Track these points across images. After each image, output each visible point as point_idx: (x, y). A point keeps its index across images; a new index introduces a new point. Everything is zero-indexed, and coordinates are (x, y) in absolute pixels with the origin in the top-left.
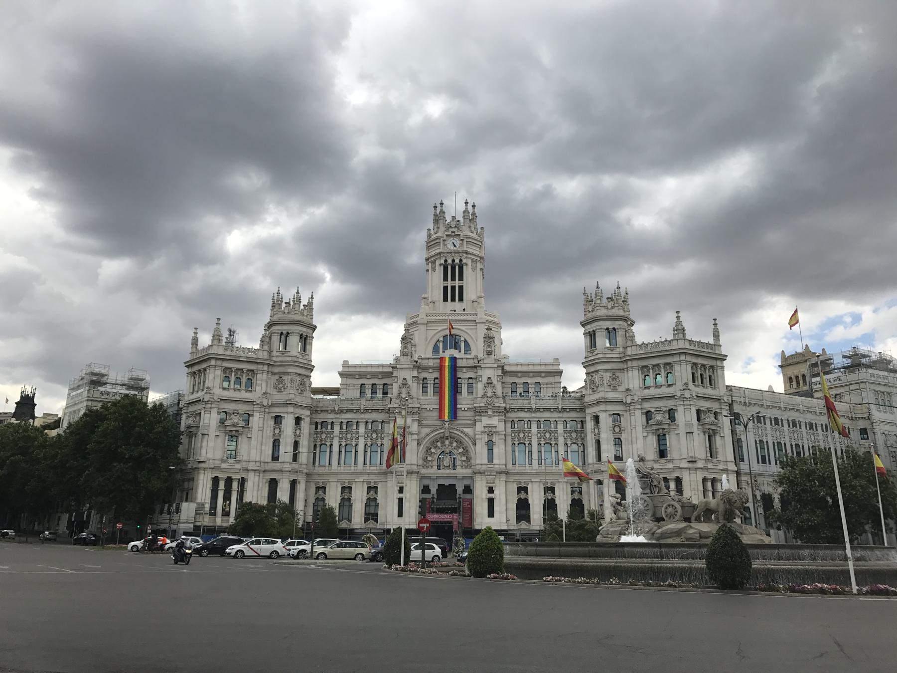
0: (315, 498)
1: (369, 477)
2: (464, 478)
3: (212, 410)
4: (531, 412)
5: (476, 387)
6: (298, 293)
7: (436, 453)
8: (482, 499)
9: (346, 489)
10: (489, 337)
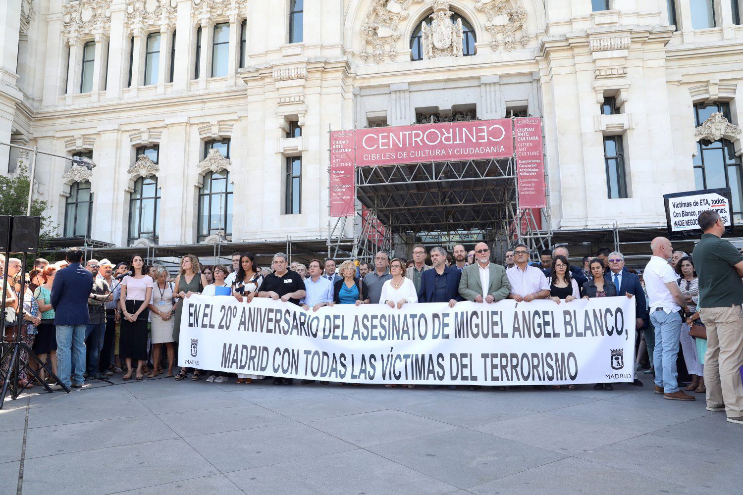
0: (65, 180)
1: (203, 109)
2: (505, 80)
7: (404, 13)
8: (581, 135)
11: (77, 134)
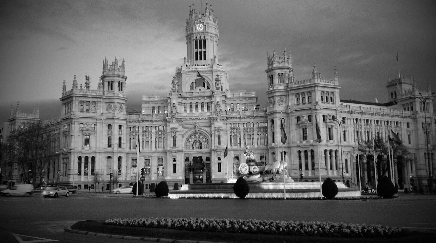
3: (75, 123)
4: (240, 119)
5: (212, 107)
6: (116, 60)
8: (215, 163)
10: (218, 80)
11: (134, 157)
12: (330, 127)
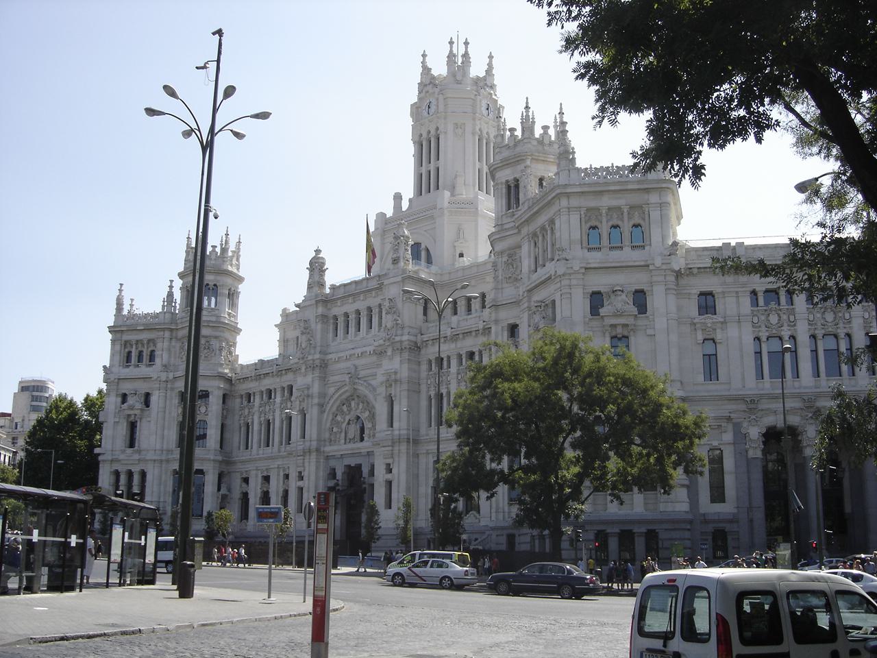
9: (267, 479)
12: (619, 331)
